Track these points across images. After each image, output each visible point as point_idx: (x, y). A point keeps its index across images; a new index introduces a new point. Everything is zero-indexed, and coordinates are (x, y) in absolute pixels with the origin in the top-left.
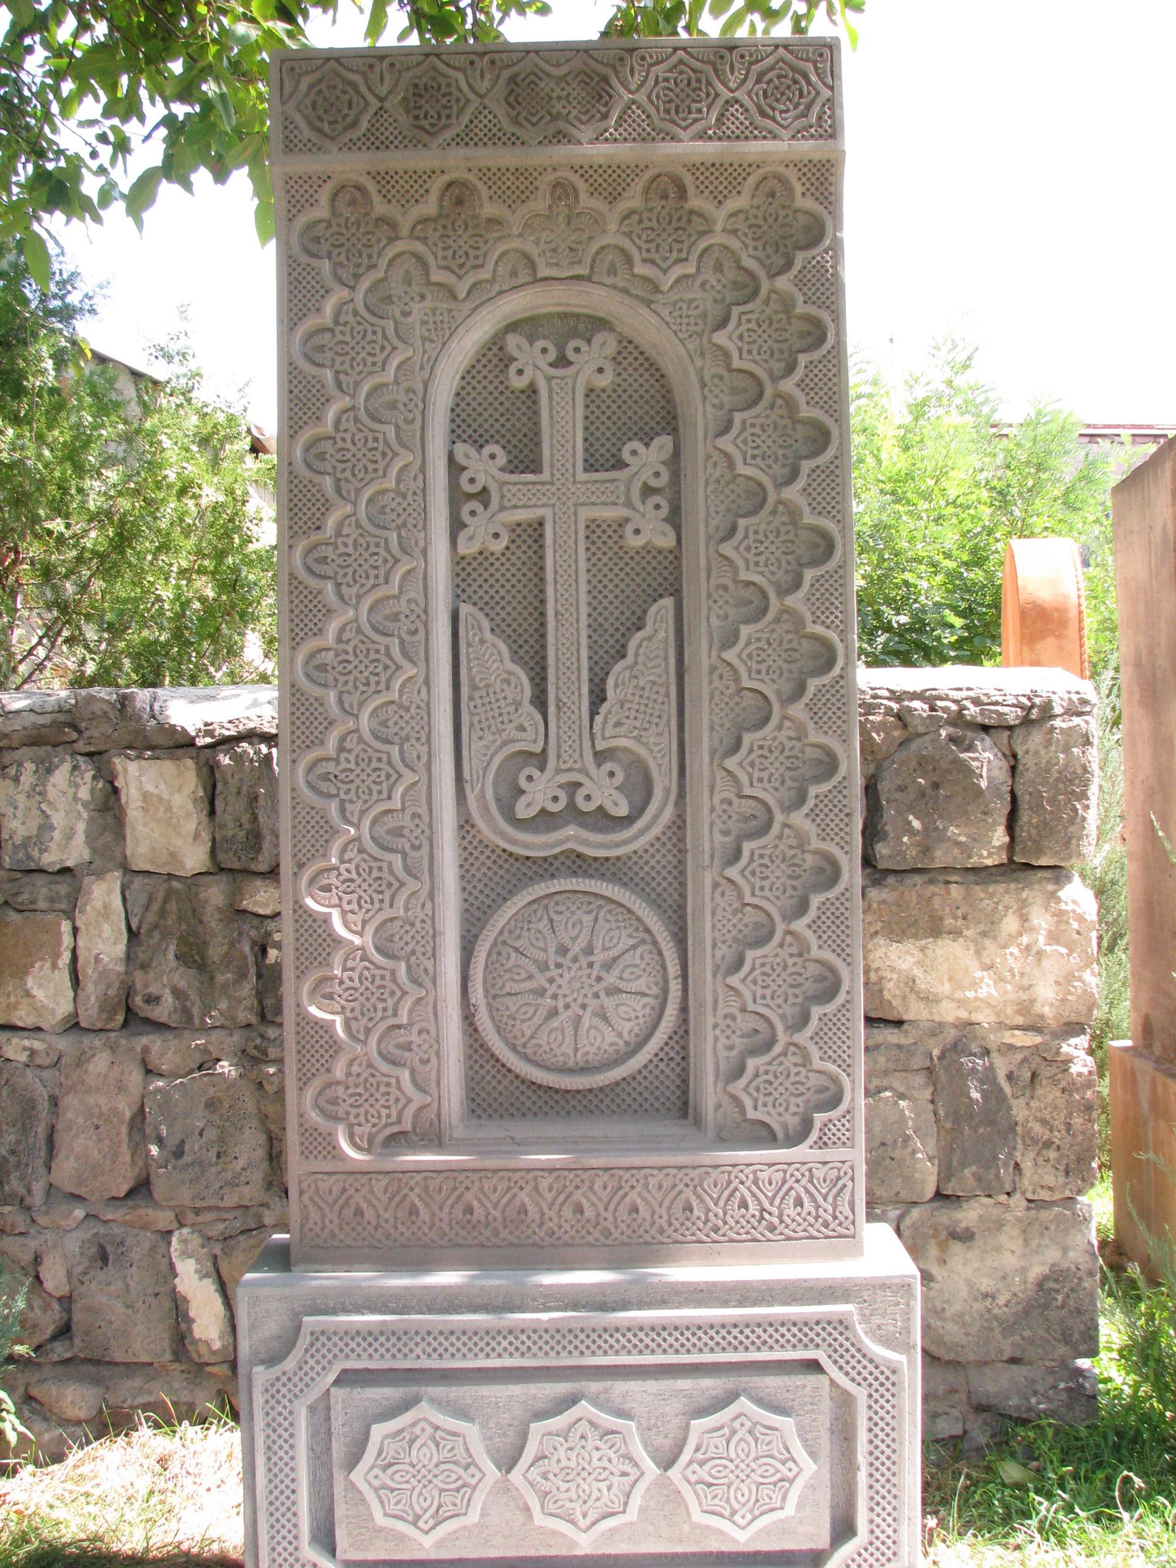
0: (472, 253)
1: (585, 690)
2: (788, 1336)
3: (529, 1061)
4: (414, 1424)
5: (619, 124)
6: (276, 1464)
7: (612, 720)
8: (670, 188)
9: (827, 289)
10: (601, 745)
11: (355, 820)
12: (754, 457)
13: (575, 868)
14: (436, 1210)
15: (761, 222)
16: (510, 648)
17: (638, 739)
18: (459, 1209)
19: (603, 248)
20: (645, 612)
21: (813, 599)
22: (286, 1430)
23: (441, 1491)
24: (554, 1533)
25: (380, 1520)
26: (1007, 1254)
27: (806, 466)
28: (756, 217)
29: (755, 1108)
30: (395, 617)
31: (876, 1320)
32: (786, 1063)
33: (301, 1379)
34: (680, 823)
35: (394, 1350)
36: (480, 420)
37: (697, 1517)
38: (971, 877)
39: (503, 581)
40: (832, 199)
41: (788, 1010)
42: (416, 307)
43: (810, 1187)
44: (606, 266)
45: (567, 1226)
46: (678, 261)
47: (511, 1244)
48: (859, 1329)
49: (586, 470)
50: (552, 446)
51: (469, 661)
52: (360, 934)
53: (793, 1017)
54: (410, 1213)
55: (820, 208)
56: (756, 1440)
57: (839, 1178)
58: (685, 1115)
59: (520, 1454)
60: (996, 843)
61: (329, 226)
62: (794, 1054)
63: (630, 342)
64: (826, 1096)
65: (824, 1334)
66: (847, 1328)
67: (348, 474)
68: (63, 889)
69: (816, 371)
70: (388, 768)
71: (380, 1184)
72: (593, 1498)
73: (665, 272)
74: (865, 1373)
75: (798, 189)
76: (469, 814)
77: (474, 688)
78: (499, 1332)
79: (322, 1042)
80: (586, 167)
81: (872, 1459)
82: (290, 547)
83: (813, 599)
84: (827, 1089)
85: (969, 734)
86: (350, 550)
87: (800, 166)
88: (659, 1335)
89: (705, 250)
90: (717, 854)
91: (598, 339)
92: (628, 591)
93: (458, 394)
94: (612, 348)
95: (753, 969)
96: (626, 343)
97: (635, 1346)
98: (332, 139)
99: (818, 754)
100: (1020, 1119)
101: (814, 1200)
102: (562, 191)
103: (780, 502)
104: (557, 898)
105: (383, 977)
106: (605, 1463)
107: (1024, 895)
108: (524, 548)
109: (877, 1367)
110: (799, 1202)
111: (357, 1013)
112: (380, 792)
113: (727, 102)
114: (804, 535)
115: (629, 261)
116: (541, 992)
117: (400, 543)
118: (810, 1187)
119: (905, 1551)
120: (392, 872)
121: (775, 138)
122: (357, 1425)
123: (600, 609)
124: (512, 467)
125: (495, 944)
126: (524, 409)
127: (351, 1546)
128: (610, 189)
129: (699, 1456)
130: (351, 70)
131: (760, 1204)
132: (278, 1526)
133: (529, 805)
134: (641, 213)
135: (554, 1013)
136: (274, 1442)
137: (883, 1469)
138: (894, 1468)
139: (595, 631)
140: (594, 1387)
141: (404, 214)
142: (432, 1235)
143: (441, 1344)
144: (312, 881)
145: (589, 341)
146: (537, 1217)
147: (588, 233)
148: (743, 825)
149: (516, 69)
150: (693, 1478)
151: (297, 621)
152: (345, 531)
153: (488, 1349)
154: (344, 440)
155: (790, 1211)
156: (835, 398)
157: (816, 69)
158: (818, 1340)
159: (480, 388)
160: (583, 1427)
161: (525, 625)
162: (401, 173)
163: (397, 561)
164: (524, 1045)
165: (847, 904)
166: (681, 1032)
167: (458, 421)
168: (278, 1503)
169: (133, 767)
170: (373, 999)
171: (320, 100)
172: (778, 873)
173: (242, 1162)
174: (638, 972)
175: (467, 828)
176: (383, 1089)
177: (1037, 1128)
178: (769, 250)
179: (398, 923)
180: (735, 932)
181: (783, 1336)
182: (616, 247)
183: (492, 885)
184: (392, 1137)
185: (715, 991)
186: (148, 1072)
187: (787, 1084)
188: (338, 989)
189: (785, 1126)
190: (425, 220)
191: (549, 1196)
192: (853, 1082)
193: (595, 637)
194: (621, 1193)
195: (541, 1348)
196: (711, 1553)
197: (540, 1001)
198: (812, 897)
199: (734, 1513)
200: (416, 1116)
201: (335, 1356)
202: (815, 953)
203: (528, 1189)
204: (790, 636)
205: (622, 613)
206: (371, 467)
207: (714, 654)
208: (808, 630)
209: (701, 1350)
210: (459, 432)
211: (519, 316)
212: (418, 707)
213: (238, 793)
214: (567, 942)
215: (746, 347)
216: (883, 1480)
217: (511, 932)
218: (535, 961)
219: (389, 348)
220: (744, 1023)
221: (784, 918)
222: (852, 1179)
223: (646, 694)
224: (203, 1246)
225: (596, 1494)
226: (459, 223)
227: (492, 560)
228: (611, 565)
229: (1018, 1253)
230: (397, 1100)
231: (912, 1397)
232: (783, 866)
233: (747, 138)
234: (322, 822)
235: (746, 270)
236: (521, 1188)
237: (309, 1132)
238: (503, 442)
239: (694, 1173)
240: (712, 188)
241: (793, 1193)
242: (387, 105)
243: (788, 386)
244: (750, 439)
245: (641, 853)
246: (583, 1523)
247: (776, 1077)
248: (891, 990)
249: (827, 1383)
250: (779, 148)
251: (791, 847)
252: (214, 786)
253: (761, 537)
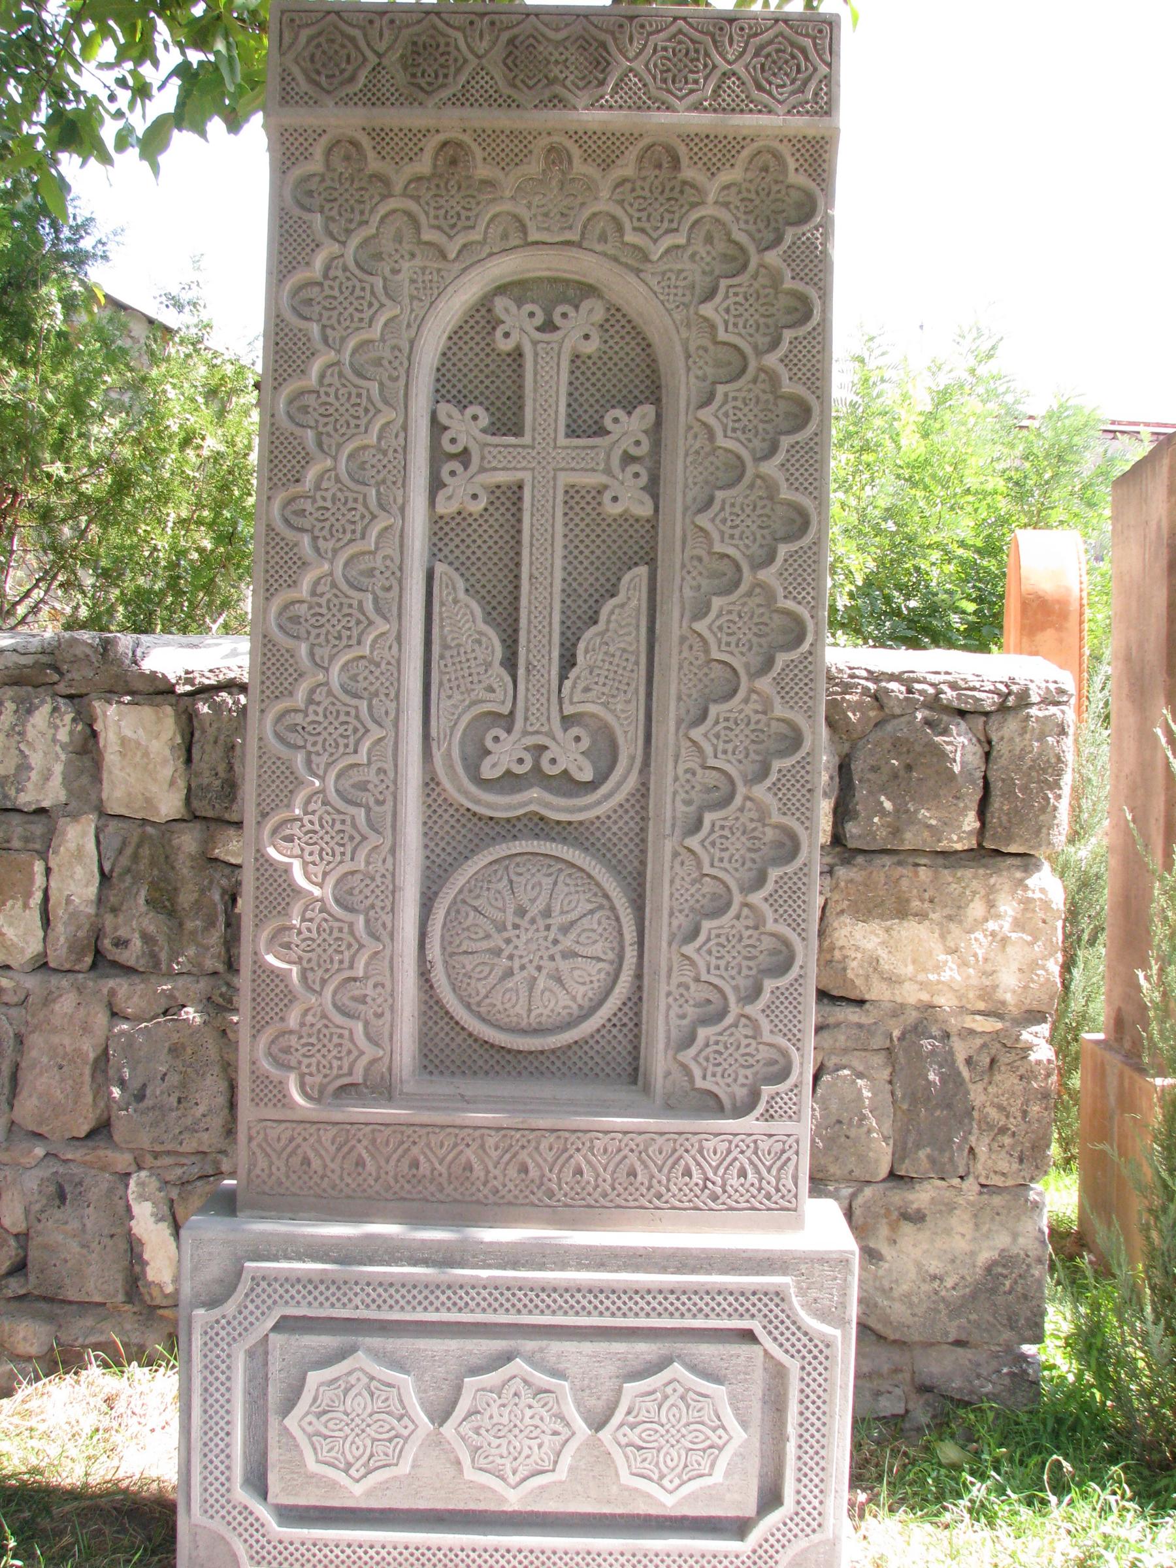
0: (464, 213)
1: (556, 654)
2: (724, 1305)
3: (484, 1020)
4: (350, 1373)
5: (615, 91)
6: (212, 1406)
7: (581, 686)
8: (664, 157)
9: (815, 267)
10: (569, 710)
11: (321, 773)
12: (734, 430)
13: (537, 831)
14: (383, 1163)
15: (753, 196)
16: (483, 609)
17: (605, 705)
18: (405, 1163)
19: (594, 215)
20: (619, 579)
21: (786, 574)
22: (223, 1373)
23: (374, 1440)
24: (483, 1488)
25: (312, 1466)
26: (958, 1237)
27: (785, 442)
28: (749, 191)
29: (704, 1078)
30: (370, 573)
31: (814, 1293)
32: (737, 1035)
33: (240, 1323)
34: (643, 792)
35: (333, 1299)
36: (465, 381)
37: (626, 1478)
38: (940, 861)
39: (479, 542)
40: (825, 176)
41: (742, 982)
42: (406, 265)
43: (754, 1158)
44: (598, 232)
45: (511, 1186)
46: (668, 231)
47: (455, 1201)
48: (796, 1301)
49: (567, 436)
50: (535, 410)
51: (442, 620)
52: (320, 885)
53: (746, 989)
54: (357, 1164)
55: (813, 185)
56: (688, 1407)
57: (783, 1151)
58: (635, 1082)
59: (453, 1408)
60: (967, 828)
61: (323, 180)
62: (745, 1026)
63: (618, 310)
64: (775, 1068)
65: (759, 1305)
66: (783, 1300)
67: (330, 428)
68: (38, 829)
69: (800, 347)
70: (355, 722)
71: (327, 1136)
72: (524, 1455)
73: (655, 241)
74: (799, 1345)
75: (792, 165)
76: (434, 772)
77: (445, 646)
78: (438, 1287)
79: (277, 991)
80: (581, 133)
81: (801, 1431)
82: (269, 498)
83: (786, 574)
84: (776, 1062)
85: (945, 718)
86: (328, 504)
87: (794, 141)
88: (596, 1297)
89: (697, 222)
90: (679, 823)
91: (586, 305)
92: (604, 559)
93: (444, 354)
94: (599, 315)
95: (708, 940)
96: (615, 311)
97: (572, 1307)
98: (328, 92)
99: (783, 729)
100: (977, 1103)
101: (758, 1172)
102: (556, 155)
103: (758, 476)
104: (518, 859)
105: (341, 930)
106: (537, 1421)
107: (992, 881)
108: (502, 510)
109: (811, 1340)
110: (743, 1173)
111: (313, 964)
112: (346, 746)
113: (724, 74)
114: (781, 510)
115: (620, 229)
116: (498, 952)
117: (379, 500)
118: (754, 1158)
119: (830, 1522)
120: (354, 825)
121: (770, 112)
122: (293, 1371)
123: (575, 574)
124: (495, 429)
125: (454, 902)
126: (509, 373)
127: (283, 1489)
128: (604, 156)
129: (630, 1419)
130: (350, 24)
131: (704, 1173)
132: (211, 1467)
133: (494, 766)
134: (634, 183)
135: (509, 973)
136: (211, 1384)
137: (812, 1441)
138: (823, 1441)
139: (569, 596)
140: (530, 1345)
141: (397, 172)
142: (377, 1187)
143: (379, 1295)
144: (275, 831)
145: (577, 307)
146: (482, 1174)
147: (580, 200)
148: (705, 796)
149: (515, 31)
150: (624, 1441)
151: (272, 572)
152: (324, 485)
153: (426, 1303)
154: (327, 394)
155: (734, 1181)
156: (818, 375)
157: (815, 45)
158: (753, 1310)
159: (466, 348)
160: (517, 1384)
161: (500, 588)
162: (396, 130)
163: (374, 517)
164: (479, 1004)
165: (805, 880)
166: (635, 999)
167: (443, 381)
168: (212, 1445)
169: (112, 710)
170: (330, 951)
171: (318, 53)
172: (738, 845)
173: (202, 1109)
174: (594, 936)
175: (432, 785)
176: (336, 1040)
177: (993, 1113)
178: (761, 225)
179: (359, 876)
180: (692, 902)
181: (719, 1304)
182: (608, 214)
183: (454, 844)
184: (343, 1088)
185: (670, 959)
186: (114, 1014)
187: (736, 1055)
188: (296, 939)
189: (733, 1097)
190: (419, 179)
191: (495, 1154)
192: (802, 1056)
193: (569, 602)
194: (566, 1155)
195: (478, 1304)
196: (638, 1516)
197: (496, 960)
198: (770, 870)
199: (662, 1477)
200: (367, 1070)
201: (275, 1302)
202: (770, 926)
203: (474, 1146)
204: (762, 610)
205: (597, 579)
206: (353, 422)
207: (684, 624)
208: (779, 605)
209: (637, 1315)
210: (444, 391)
211: (508, 280)
212: (389, 663)
213: (215, 742)
214: (526, 903)
215: (732, 320)
216: (811, 1452)
217: (470, 891)
218: (493, 921)
219: (376, 305)
220: (698, 993)
221: (742, 890)
222: (797, 1153)
223: (616, 660)
224: (160, 1189)
225: (526, 1451)
226: (452, 183)
227: (470, 520)
228: (588, 530)
229: (968, 1237)
230: (349, 1052)
231: (845, 1372)
232: (743, 839)
233: (742, 111)
234: (287, 773)
235: (736, 243)
236: (468, 1145)
237: (260, 1078)
238: (487, 403)
239: (639, 1139)
240: (705, 159)
241: (737, 1164)
242: (385, 62)
243: (771, 360)
244: (731, 412)
245: (603, 818)
246: (513, 1480)
247: (726, 1048)
248: (855, 970)
249: (762, 1353)
250: (774, 123)
251: (752, 820)
252: (192, 734)
253: (737, 510)
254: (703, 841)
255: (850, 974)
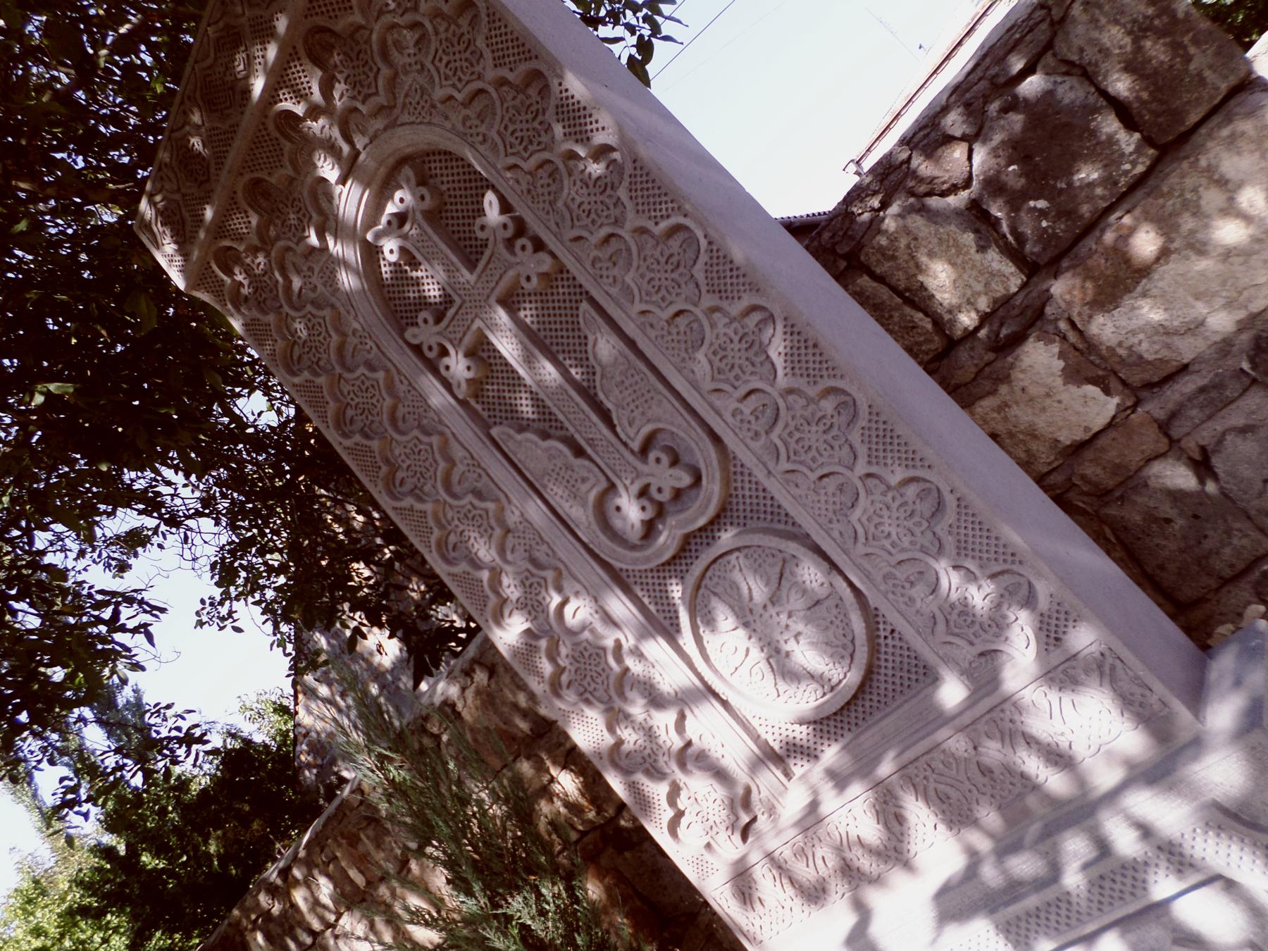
10: (636, 445)
12: (525, 149)
21: (640, 207)
90: (765, 458)
107: (1203, 163)
215: (455, 80)
232: (814, 428)
242: (183, 190)
254: (789, 458)
255: (1149, 357)
